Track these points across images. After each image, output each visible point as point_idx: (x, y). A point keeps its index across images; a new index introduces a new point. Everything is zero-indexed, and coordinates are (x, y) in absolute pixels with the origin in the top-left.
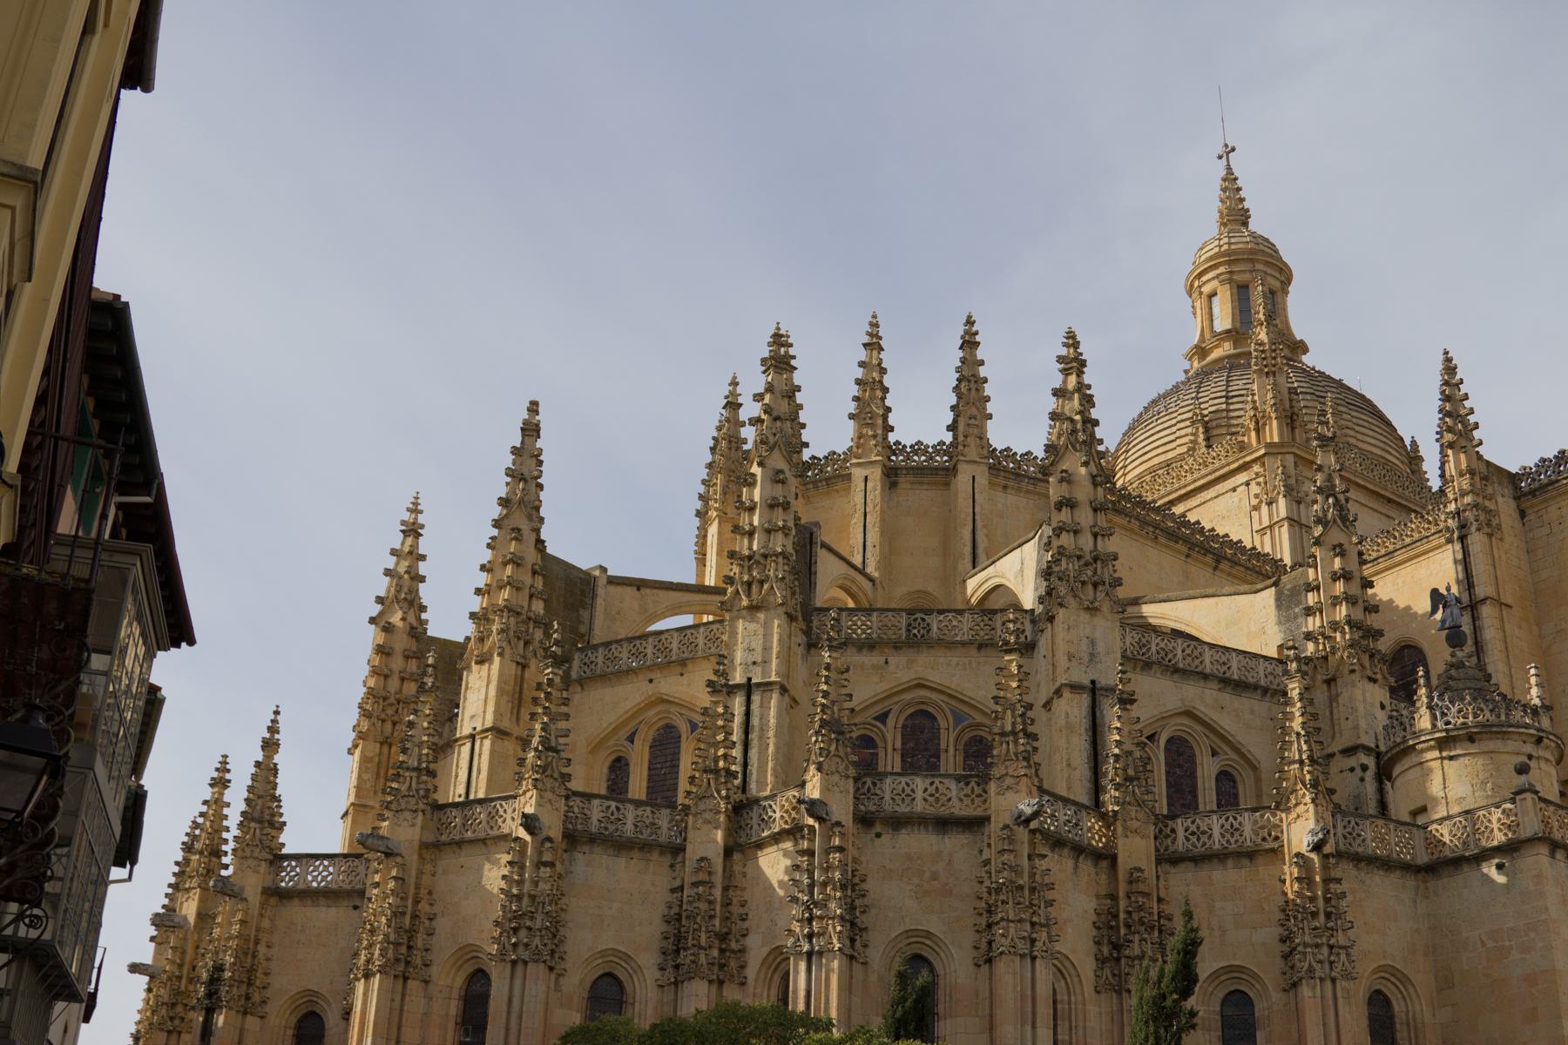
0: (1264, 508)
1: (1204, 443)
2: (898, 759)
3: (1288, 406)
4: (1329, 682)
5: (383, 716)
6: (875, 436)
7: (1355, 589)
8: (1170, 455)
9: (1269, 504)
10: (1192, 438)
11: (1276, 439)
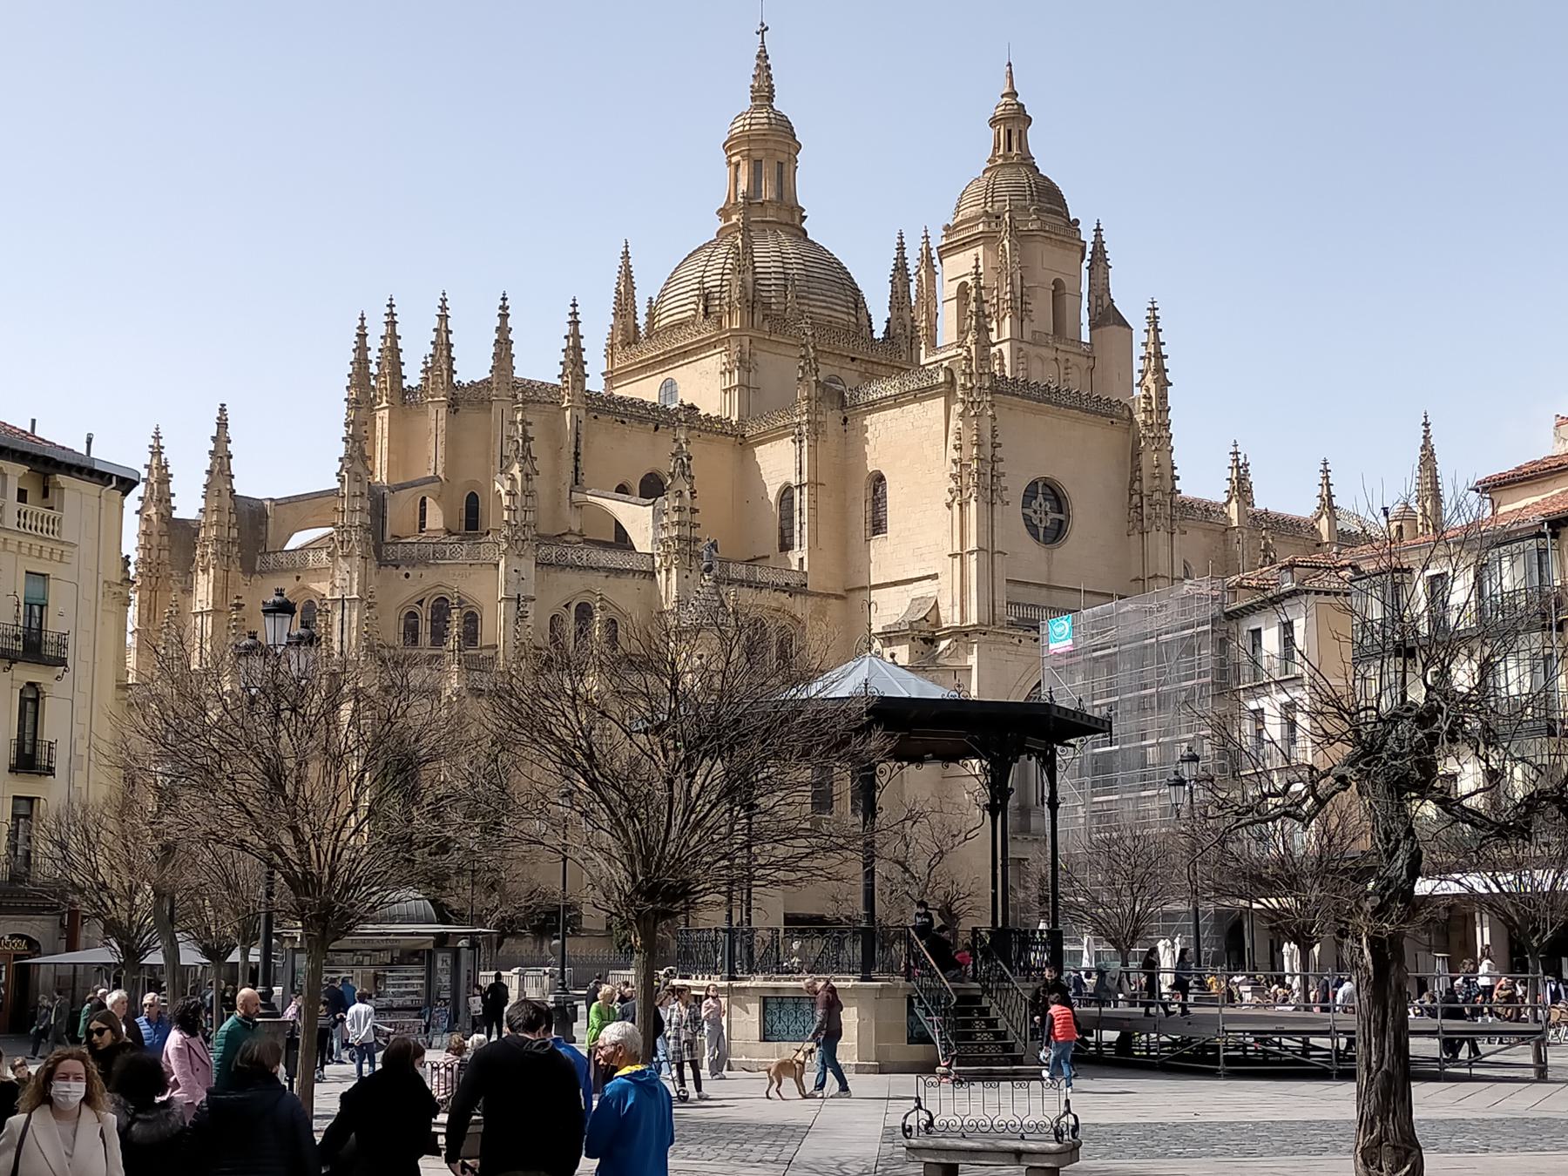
0: (728, 374)
1: (702, 312)
2: (429, 623)
3: (751, 297)
4: (668, 571)
5: (150, 574)
6: (442, 383)
7: (686, 516)
8: (684, 315)
9: (730, 373)
10: (693, 306)
11: (738, 326)
